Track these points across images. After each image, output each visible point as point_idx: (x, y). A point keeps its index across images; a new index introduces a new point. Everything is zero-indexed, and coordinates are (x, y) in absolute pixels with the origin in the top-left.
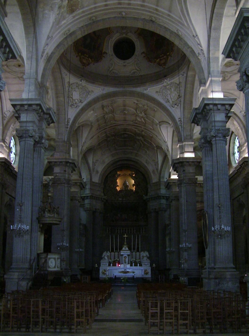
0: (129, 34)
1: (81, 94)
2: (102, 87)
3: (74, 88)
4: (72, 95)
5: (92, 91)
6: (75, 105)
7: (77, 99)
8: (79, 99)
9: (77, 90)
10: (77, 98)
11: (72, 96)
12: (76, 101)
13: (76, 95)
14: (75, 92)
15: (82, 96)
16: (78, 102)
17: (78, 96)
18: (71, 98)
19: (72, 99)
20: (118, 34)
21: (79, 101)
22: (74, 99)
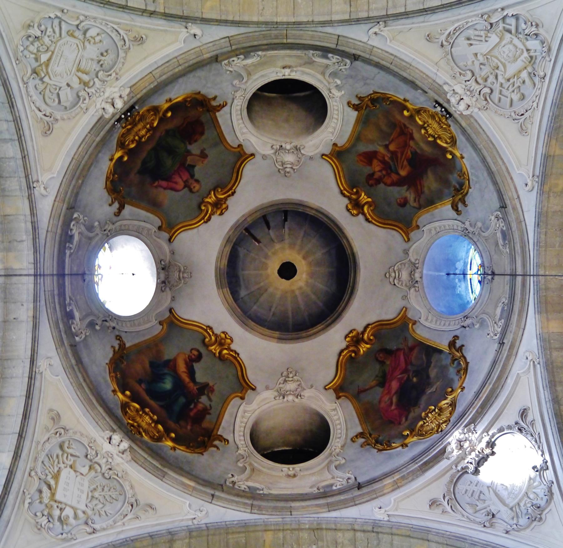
0: (307, 393)
1: (96, 494)
2: (197, 502)
3: (70, 451)
4: (56, 477)
5: (151, 506)
6: (58, 524)
7: (75, 509)
8: (84, 512)
9: (85, 470)
10: (74, 504)
11: (52, 482)
12: (68, 512)
13: (72, 489)
14: (72, 471)
15: (101, 506)
16: (72, 521)
17: (84, 496)
18: (49, 487)
19: (53, 495)
20: (269, 394)
21: (82, 521)
22: (59, 502)
